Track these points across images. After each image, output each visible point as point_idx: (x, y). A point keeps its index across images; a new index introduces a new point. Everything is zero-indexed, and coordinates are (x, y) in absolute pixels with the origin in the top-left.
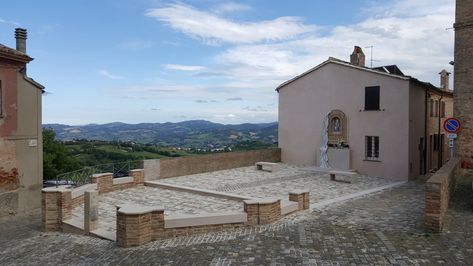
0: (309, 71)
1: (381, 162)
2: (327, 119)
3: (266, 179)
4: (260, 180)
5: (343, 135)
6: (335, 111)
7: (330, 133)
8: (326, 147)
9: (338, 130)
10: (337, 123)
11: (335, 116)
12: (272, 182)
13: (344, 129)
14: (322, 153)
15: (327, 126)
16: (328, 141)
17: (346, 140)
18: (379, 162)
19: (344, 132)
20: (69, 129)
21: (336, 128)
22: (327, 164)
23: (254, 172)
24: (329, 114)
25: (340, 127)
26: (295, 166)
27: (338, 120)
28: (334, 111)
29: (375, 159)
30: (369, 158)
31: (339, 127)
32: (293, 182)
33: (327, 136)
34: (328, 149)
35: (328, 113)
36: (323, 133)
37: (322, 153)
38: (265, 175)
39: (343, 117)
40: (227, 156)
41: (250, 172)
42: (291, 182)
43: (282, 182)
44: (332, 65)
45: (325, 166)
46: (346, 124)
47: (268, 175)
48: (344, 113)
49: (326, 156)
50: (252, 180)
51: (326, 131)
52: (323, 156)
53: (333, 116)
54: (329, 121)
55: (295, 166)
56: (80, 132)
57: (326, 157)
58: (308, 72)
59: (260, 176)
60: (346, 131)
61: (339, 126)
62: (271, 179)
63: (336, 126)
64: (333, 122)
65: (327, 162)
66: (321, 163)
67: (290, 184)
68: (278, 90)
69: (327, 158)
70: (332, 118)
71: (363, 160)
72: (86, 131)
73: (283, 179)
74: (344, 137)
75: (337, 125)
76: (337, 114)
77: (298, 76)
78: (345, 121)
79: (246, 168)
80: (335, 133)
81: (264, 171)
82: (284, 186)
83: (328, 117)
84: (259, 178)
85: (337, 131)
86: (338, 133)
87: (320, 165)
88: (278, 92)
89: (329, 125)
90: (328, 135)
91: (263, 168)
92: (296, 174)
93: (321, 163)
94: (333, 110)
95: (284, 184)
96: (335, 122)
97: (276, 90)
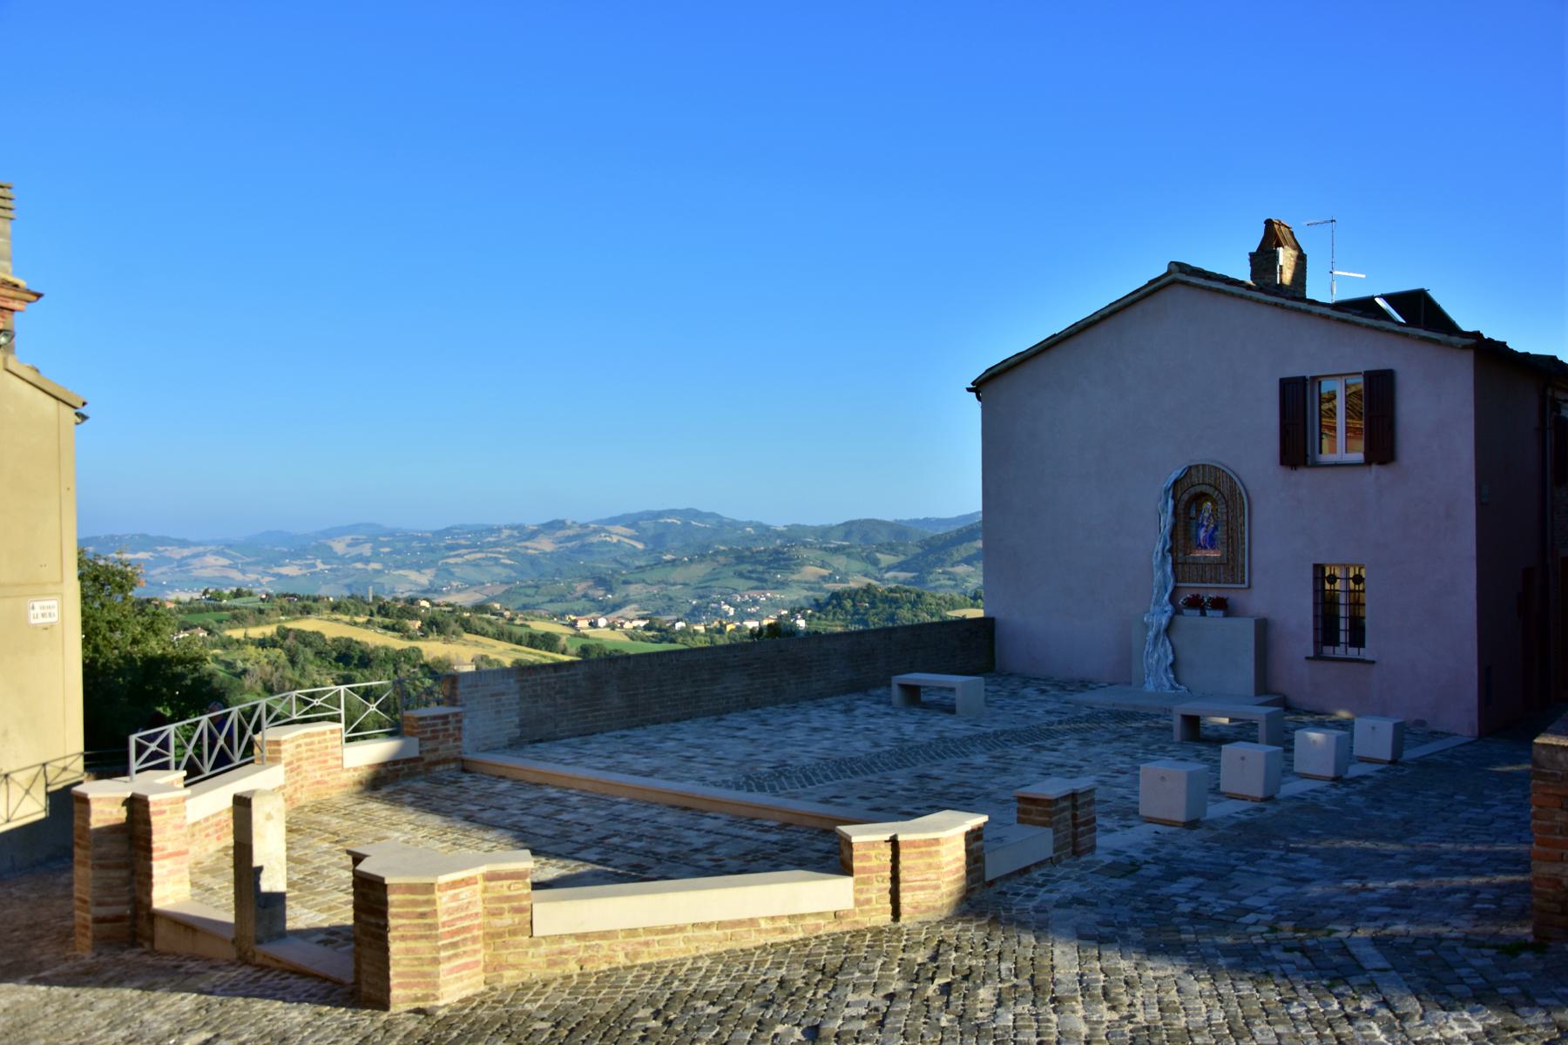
0: (1097, 317)
1: (1373, 662)
2: (1167, 502)
3: (933, 742)
4: (910, 744)
5: (1231, 563)
6: (1198, 471)
7: (1180, 555)
8: (1166, 609)
9: (1211, 542)
10: (1206, 515)
11: (1199, 489)
12: (956, 750)
14: (1151, 634)
17: (1243, 582)
18: (1367, 666)
19: (1233, 552)
20: (186, 552)
21: (1202, 534)
22: (1172, 676)
23: (887, 714)
24: (1176, 482)
25: (1217, 533)
26: (1048, 688)
27: (1209, 504)
28: (1194, 472)
29: (1353, 652)
30: (1328, 650)
31: (1213, 532)
32: (1039, 749)
33: (1169, 569)
34: (1178, 618)
35: (1173, 477)
38: (932, 726)
39: (1226, 493)
40: (781, 651)
41: (872, 712)
42: (1029, 750)
43: (998, 752)
44: (1181, 290)
46: (1240, 520)
47: (942, 723)
49: (1167, 642)
50: (876, 745)
51: (1168, 547)
52: (1155, 644)
53: (1193, 491)
54: (1175, 507)
55: (1048, 688)
56: (227, 562)
57: (1166, 651)
58: (1091, 319)
59: (909, 729)
61: (1216, 528)
62: (952, 740)
63: (1203, 530)
64: (1193, 513)
65: (1169, 671)
66: (1146, 671)
67: (1025, 759)
68: (978, 387)
70: (1186, 497)
71: (1307, 658)
72: (248, 560)
73: (1002, 738)
74: (1233, 568)
75: (1205, 523)
76: (1207, 481)
77: (1055, 335)
79: (855, 696)
80: (1199, 554)
81: (926, 706)
82: (1005, 766)
83: (1171, 492)
84: (906, 737)
85: (1206, 548)
86: (1213, 554)
87: (1145, 682)
88: (979, 398)
89: (1174, 527)
90: (1174, 565)
91: (924, 698)
92: (1053, 718)
93: (1146, 671)
95: (1002, 760)
96: (1199, 511)
97: (969, 390)
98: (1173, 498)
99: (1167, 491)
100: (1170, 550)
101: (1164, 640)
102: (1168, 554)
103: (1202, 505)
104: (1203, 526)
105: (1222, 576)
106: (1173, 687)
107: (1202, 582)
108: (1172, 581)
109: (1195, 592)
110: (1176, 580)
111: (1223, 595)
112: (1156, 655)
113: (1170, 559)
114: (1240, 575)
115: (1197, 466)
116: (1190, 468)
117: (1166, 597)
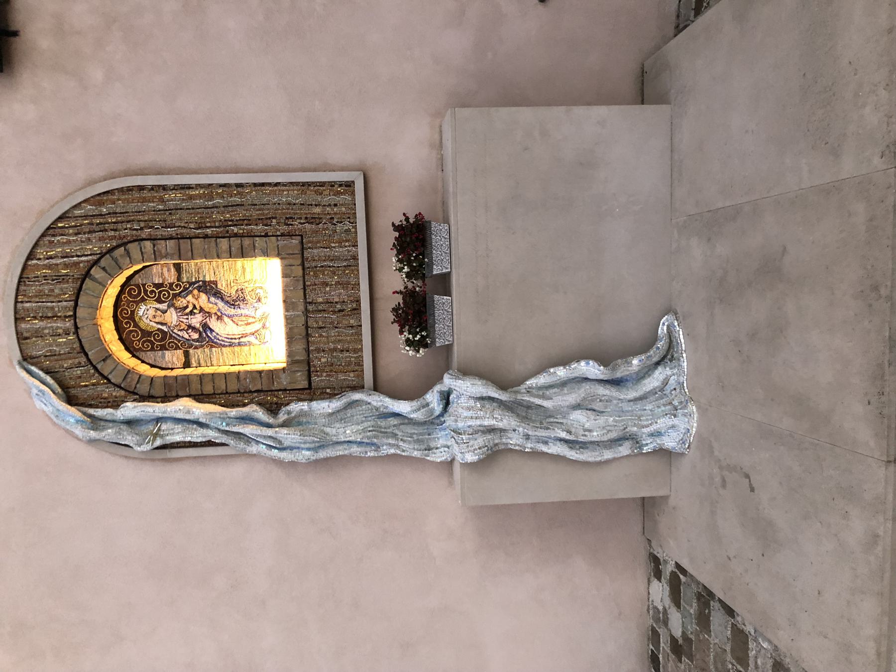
2: (130, 423)
6: (39, 334)
10: (172, 317)
13: (225, 224)
15: (199, 410)
16: (376, 388)
17: (349, 185)
24: (71, 400)
27: (142, 310)
28: (38, 348)
33: (323, 407)
36: (286, 456)
37: (514, 440)
45: (666, 382)
48: (50, 230)
49: (541, 380)
51: (260, 414)
60: (253, 196)
63: (213, 323)
69: (561, 372)
74: (314, 220)
78: (132, 207)
90: (310, 393)
93: (625, 450)
94: (25, 359)
98: (116, 404)
99: (96, 423)
100: (273, 409)
101: (529, 391)
102: (282, 417)
103: (146, 333)
104: (206, 327)
105: (338, 251)
106: (668, 356)
107: (357, 310)
108: (357, 396)
109: (386, 316)
110: (358, 387)
111: (387, 238)
112: (578, 417)
113: (296, 407)
114: (328, 199)
115: (21, 338)
116: (27, 359)
117: (403, 407)
